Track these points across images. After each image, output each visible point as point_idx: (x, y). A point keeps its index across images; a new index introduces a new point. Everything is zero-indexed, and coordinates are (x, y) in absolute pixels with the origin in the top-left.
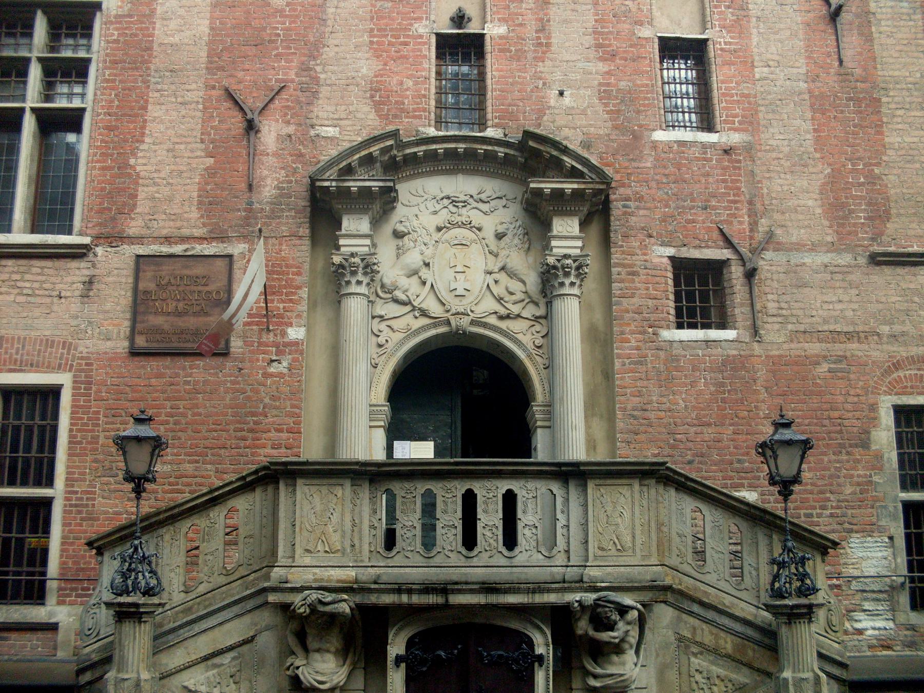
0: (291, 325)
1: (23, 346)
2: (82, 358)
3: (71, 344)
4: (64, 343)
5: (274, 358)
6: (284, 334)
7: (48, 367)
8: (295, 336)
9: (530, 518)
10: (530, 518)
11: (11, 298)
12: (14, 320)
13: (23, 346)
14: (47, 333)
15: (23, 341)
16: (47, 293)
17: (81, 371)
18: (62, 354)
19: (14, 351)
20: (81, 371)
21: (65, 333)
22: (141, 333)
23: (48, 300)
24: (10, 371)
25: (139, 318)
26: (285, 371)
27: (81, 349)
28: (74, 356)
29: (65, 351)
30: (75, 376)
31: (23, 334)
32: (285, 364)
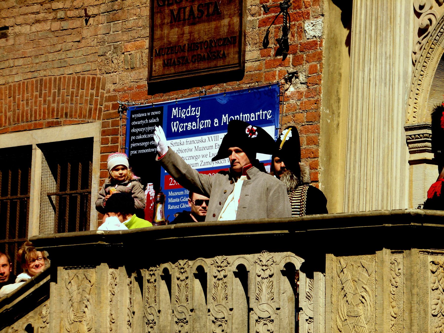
0: (307, 16)
1: (59, 90)
2: (110, 99)
3: (99, 79)
4: (93, 79)
5: (291, 70)
6: (302, 31)
7: (80, 116)
8: (312, 33)
9: (265, 307)
10: (265, 307)
11: (46, 26)
12: (51, 56)
13: (59, 90)
14: (78, 69)
15: (58, 82)
16: (76, 13)
17: (109, 117)
18: (92, 95)
19: (51, 98)
20: (109, 117)
21: (93, 66)
22: (158, 55)
23: (77, 23)
24: (50, 125)
25: (158, 33)
26: (303, 88)
27: (110, 86)
28: (102, 97)
29: (94, 92)
30: (103, 125)
31: (57, 72)
32: (302, 78)
